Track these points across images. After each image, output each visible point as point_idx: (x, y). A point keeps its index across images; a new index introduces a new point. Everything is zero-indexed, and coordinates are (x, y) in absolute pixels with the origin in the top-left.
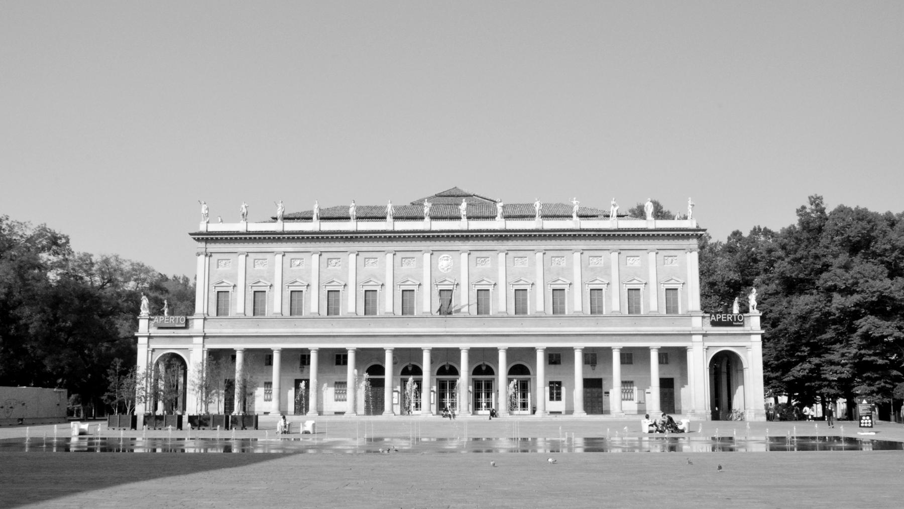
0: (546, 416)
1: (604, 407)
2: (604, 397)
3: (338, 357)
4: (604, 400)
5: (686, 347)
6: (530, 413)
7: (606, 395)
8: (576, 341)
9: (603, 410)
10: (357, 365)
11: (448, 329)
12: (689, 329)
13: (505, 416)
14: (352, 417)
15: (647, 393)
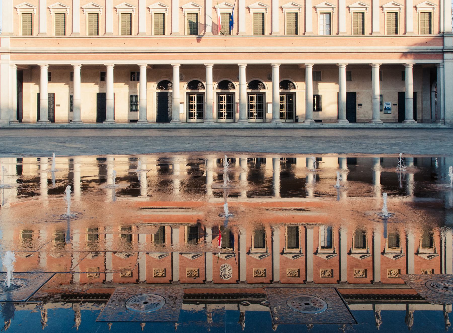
0: (313, 124)
1: (357, 116)
2: (357, 108)
3: (132, 73)
4: (357, 111)
5: (439, 63)
6: (294, 121)
7: (359, 106)
8: (341, 58)
9: (357, 119)
10: (150, 79)
11: (227, 48)
12: (441, 47)
13: (277, 124)
14: (143, 124)
15: (396, 105)
